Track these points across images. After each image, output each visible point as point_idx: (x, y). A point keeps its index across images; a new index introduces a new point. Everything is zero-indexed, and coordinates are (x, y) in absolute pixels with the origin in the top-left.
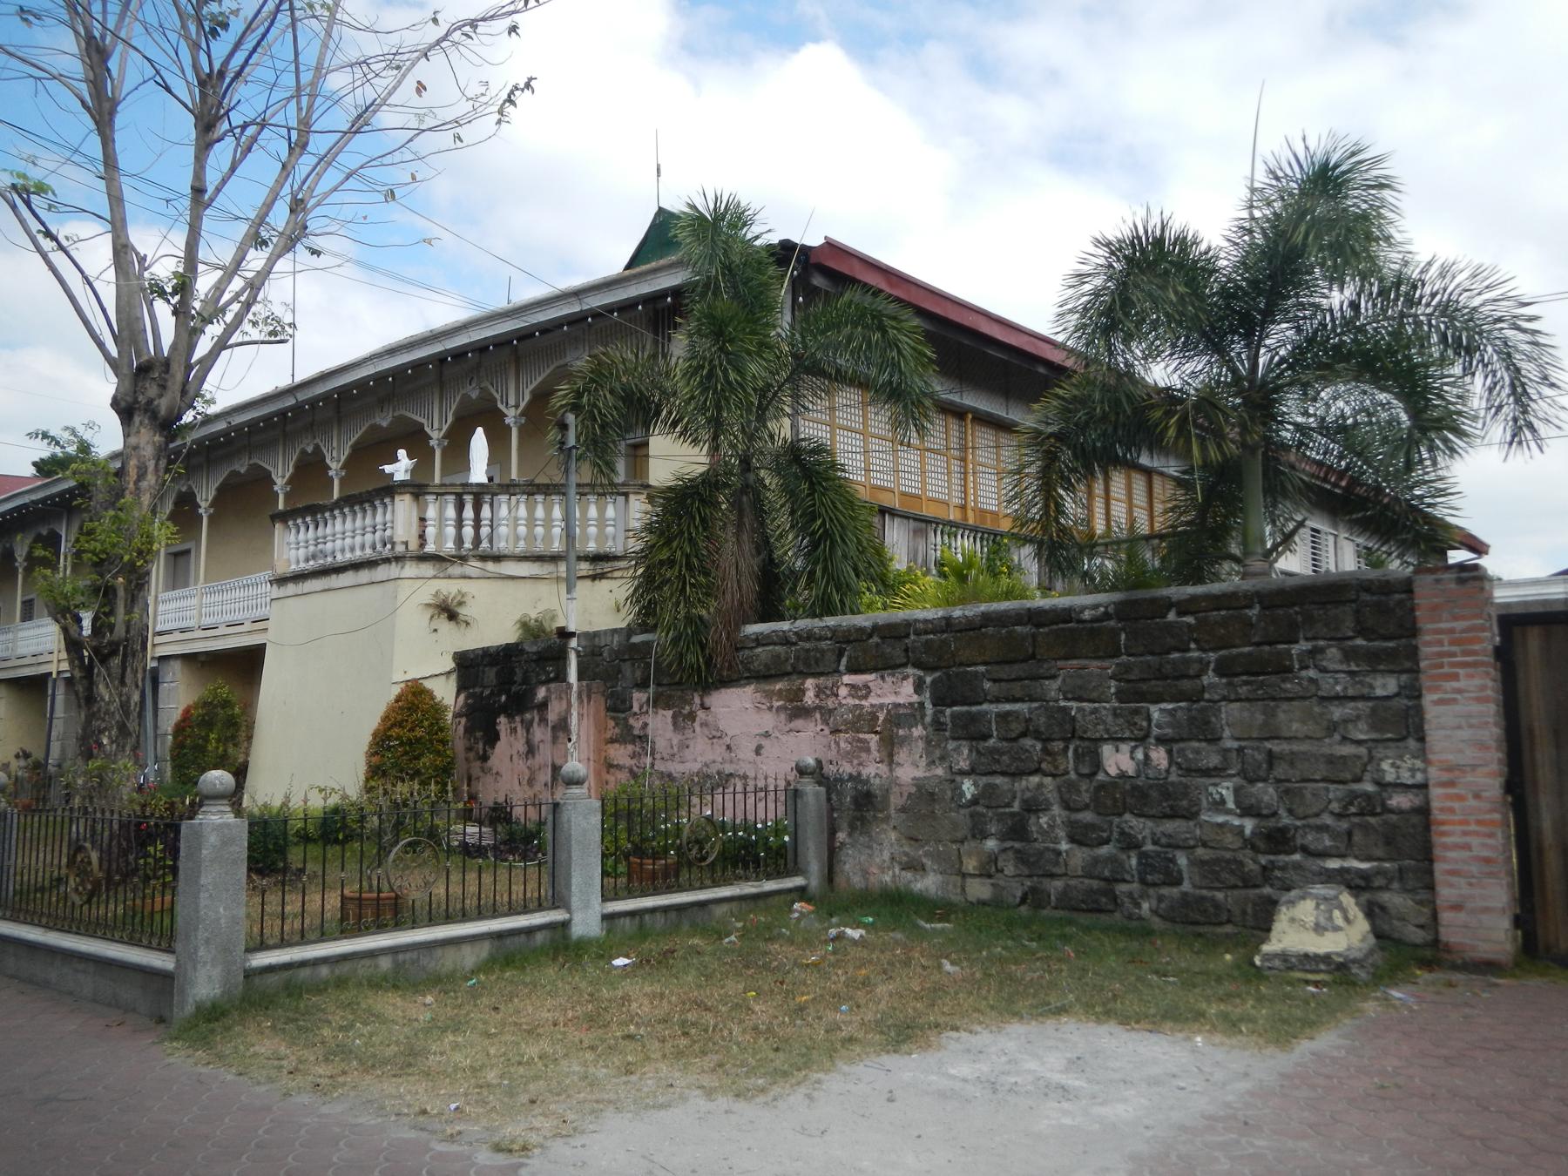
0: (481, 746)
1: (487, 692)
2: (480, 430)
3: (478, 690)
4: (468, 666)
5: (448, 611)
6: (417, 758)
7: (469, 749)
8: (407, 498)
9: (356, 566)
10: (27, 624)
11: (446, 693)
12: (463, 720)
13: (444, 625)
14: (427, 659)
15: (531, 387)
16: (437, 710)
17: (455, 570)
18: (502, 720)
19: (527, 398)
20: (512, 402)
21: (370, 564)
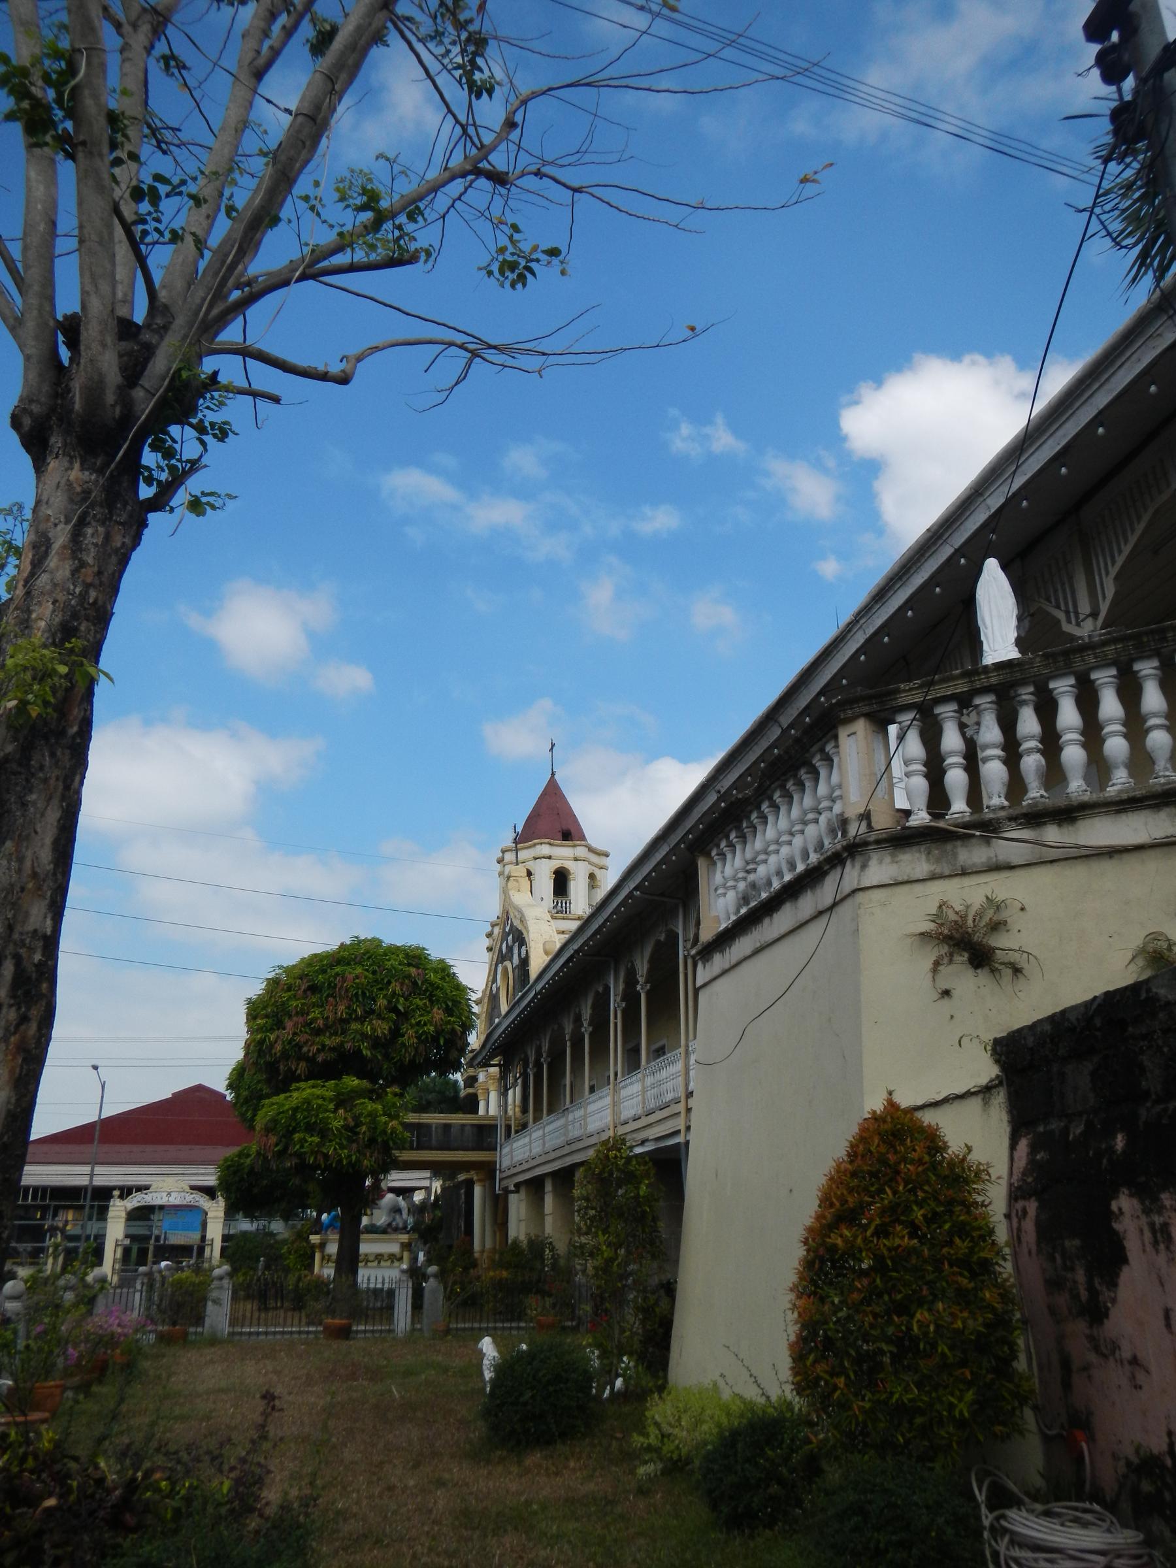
0: (1080, 1276)
1: (1077, 1129)
2: (992, 565)
3: (1055, 1125)
4: (1029, 1065)
5: (969, 946)
6: (903, 1309)
7: (1054, 1284)
8: (861, 727)
9: (792, 891)
10: (594, 1096)
11: (981, 1139)
12: (1032, 1206)
13: (966, 982)
14: (931, 1056)
15: (1114, 571)
16: (959, 1178)
17: (975, 854)
18: (1125, 1203)
19: (1110, 590)
20: (1085, 608)
21: (811, 878)
